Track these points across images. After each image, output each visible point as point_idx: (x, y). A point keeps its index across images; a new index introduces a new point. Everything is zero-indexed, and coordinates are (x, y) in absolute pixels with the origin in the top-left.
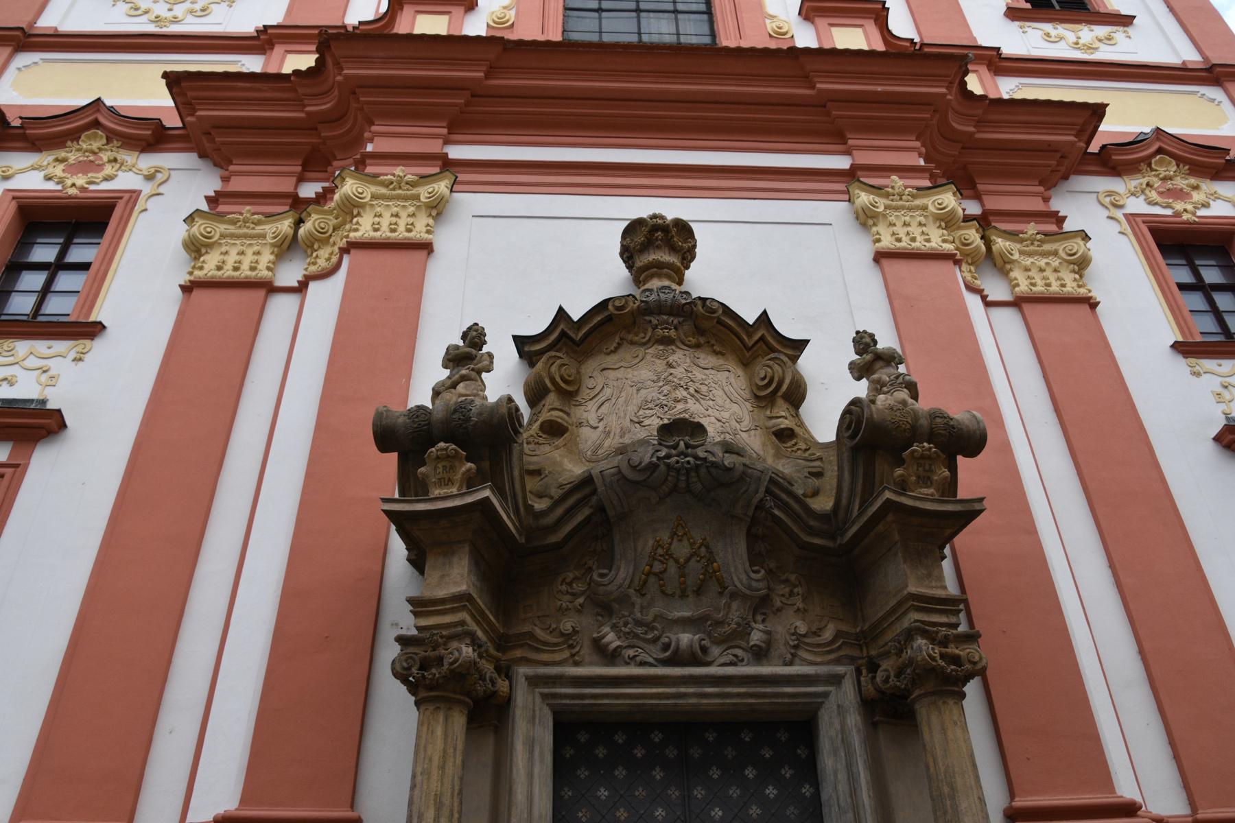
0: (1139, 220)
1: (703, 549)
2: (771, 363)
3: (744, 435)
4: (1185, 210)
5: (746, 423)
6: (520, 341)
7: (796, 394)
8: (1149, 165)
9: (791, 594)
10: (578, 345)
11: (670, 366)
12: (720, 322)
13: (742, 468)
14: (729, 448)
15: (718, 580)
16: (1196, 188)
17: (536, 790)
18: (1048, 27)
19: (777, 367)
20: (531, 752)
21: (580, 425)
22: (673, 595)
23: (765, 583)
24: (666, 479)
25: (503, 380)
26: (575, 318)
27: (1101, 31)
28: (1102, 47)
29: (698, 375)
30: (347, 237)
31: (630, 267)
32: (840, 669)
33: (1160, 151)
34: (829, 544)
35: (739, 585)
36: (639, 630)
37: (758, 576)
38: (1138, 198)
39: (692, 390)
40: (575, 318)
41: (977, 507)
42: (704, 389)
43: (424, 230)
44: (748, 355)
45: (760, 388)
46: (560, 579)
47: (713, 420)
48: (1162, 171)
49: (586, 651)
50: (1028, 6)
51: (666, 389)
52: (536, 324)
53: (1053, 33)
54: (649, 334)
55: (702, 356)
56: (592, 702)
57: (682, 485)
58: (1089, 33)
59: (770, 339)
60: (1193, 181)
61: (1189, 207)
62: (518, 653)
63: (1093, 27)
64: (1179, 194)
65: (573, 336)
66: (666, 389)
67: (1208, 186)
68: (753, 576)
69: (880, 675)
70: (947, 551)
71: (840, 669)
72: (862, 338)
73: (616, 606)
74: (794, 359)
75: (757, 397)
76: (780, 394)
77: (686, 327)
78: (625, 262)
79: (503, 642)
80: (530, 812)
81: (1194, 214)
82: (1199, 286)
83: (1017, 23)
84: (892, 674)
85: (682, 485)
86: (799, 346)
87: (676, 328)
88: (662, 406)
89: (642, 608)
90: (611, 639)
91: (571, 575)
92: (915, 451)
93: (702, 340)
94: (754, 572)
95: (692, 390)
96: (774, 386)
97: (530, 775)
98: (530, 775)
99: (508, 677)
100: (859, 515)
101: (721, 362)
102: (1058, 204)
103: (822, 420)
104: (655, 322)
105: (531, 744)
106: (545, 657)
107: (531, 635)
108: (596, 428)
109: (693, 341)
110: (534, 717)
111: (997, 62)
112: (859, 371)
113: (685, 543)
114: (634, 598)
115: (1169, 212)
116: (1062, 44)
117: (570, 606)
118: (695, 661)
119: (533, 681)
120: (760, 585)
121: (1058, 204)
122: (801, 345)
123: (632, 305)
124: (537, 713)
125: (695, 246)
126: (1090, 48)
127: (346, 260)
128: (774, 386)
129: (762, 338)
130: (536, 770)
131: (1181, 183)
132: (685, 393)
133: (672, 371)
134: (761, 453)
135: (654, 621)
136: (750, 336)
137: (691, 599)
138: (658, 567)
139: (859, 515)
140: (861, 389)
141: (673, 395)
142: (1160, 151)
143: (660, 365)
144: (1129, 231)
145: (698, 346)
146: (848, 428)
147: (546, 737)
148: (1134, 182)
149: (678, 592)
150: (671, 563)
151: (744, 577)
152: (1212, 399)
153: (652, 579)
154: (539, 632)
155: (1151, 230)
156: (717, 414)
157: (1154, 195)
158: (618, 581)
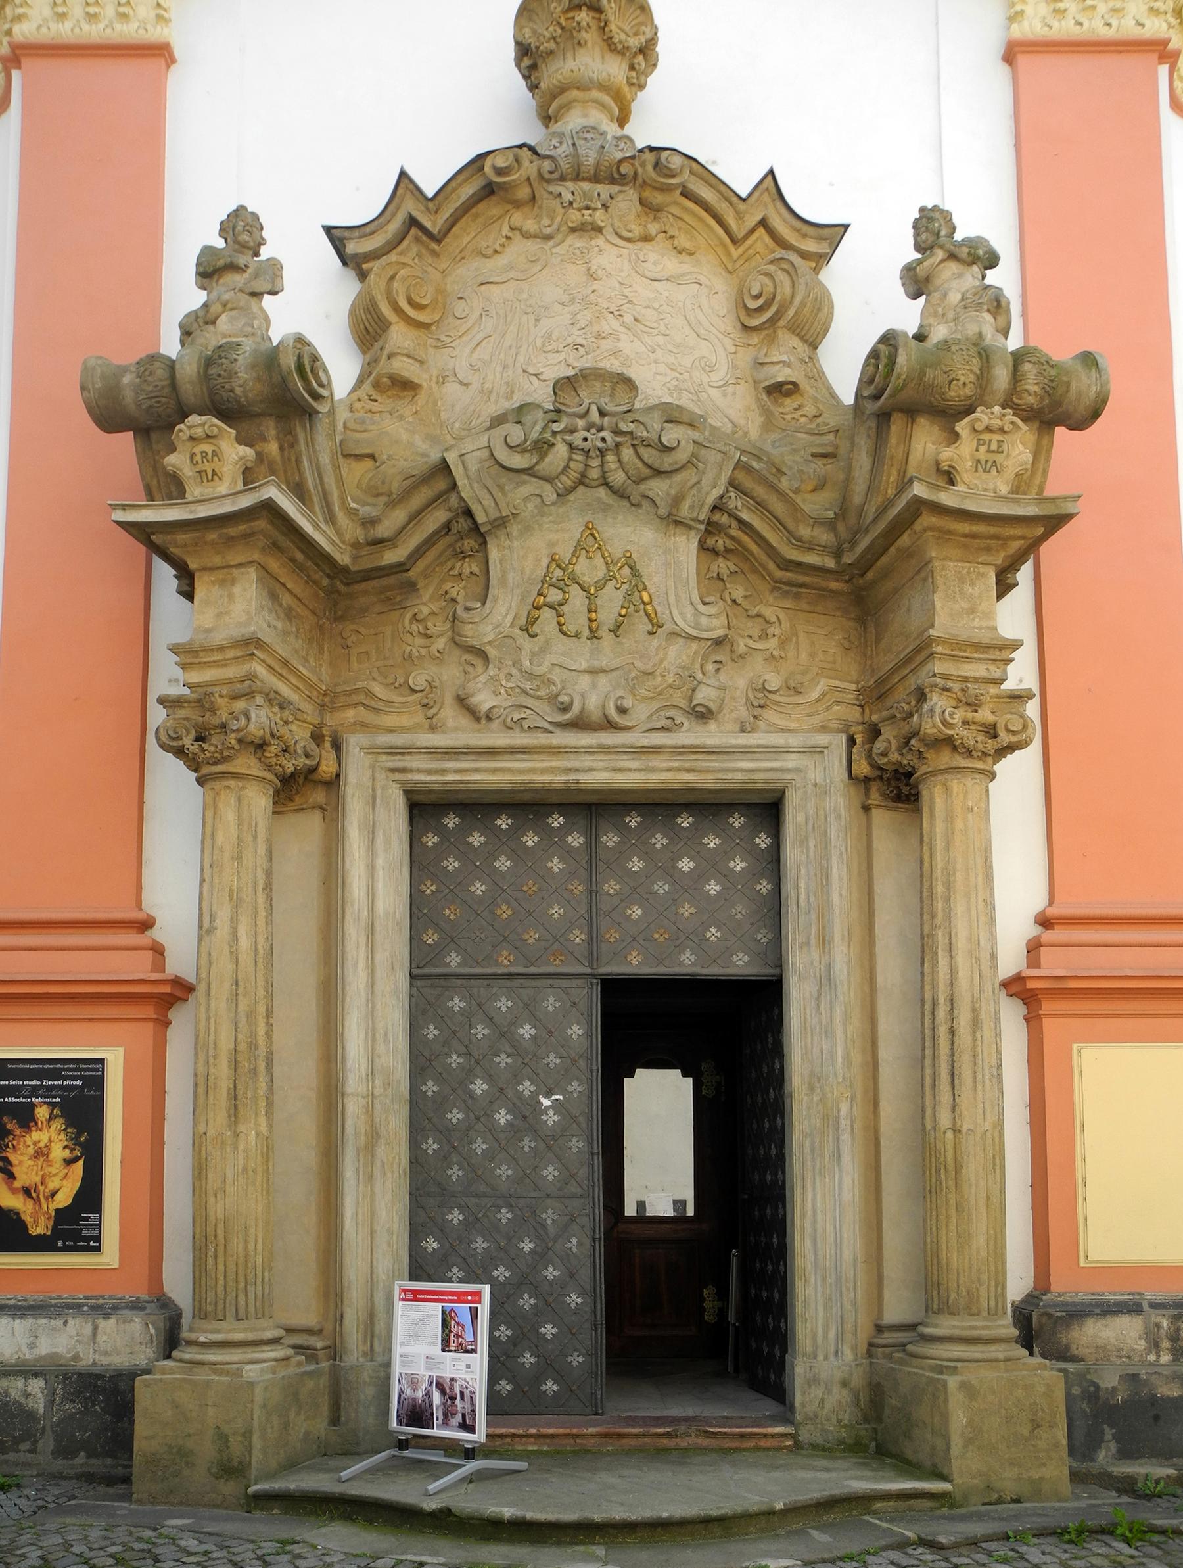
1: (626, 570)
2: (772, 268)
3: (714, 393)
5: (718, 377)
6: (336, 236)
7: (811, 326)
9: (764, 636)
10: (439, 242)
11: (592, 277)
12: (686, 194)
13: (691, 448)
14: (673, 416)
15: (647, 615)
17: (380, 886)
19: (781, 277)
20: (372, 841)
21: (442, 380)
22: (577, 635)
23: (723, 618)
24: (567, 466)
25: (309, 306)
26: (430, 193)
29: (642, 290)
30: (9, 33)
31: (533, 88)
32: (822, 739)
34: (830, 563)
35: (681, 624)
36: (528, 686)
37: (712, 610)
39: (628, 318)
40: (430, 193)
41: (1070, 508)
42: (650, 315)
43: (152, 14)
44: (735, 252)
45: (750, 312)
46: (409, 616)
47: (662, 368)
49: (449, 713)
51: (585, 316)
52: (362, 204)
54: (559, 219)
55: (652, 257)
56: (458, 777)
57: (594, 474)
59: (779, 224)
62: (350, 714)
65: (428, 225)
66: (585, 316)
68: (701, 608)
69: (879, 745)
70: (1025, 574)
71: (822, 739)
72: (931, 219)
73: (492, 652)
74: (822, 259)
75: (745, 328)
76: (782, 323)
77: (623, 205)
78: (524, 77)
79: (328, 701)
80: (372, 909)
84: (894, 744)
85: (594, 474)
86: (835, 233)
87: (605, 207)
88: (577, 347)
89: (533, 654)
90: (484, 700)
91: (425, 610)
92: (978, 420)
93: (653, 228)
94: (704, 604)
95: (628, 318)
96: (774, 309)
97: (371, 868)
98: (371, 868)
99: (337, 746)
100: (876, 520)
101: (686, 267)
103: (842, 367)
104: (567, 196)
105: (371, 832)
106: (390, 720)
107: (369, 693)
108: (466, 385)
109: (637, 230)
110: (374, 798)
112: (916, 282)
113: (599, 561)
114: (520, 641)
117: (423, 651)
118: (610, 725)
119: (374, 751)
120: (715, 622)
122: (835, 233)
123: (529, 167)
124: (379, 792)
125: (652, 41)
127: (16, 75)
128: (774, 309)
129: (763, 223)
130: (380, 862)
132: (615, 324)
133: (596, 285)
134: (742, 422)
135: (550, 671)
136: (739, 216)
137: (607, 639)
138: (554, 596)
139: (876, 520)
140: (907, 316)
141: (596, 328)
143: (574, 274)
145: (646, 238)
146: (871, 381)
147: (394, 821)
149: (586, 633)
150: (575, 590)
151: (689, 612)
153: (547, 613)
154: (378, 689)
156: (671, 359)
158: (497, 617)
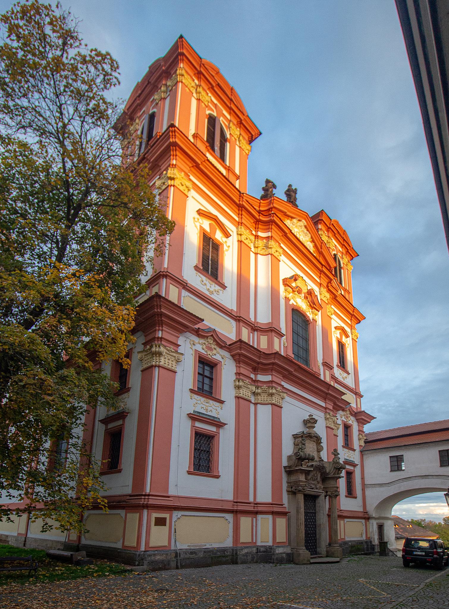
18: (204, 278)
27: (218, 288)
28: (215, 294)
38: (200, 346)
48: (209, 341)
50: (202, 268)
53: (205, 282)
58: (215, 287)
60: (215, 347)
61: (211, 354)
63: (216, 286)
64: (210, 349)
67: (218, 349)
102: (181, 341)
115: (206, 353)
116: (205, 287)
121: (181, 341)
126: (212, 293)
131: (213, 346)
142: (212, 335)
148: (202, 341)
155: (199, 356)
157: (204, 347)
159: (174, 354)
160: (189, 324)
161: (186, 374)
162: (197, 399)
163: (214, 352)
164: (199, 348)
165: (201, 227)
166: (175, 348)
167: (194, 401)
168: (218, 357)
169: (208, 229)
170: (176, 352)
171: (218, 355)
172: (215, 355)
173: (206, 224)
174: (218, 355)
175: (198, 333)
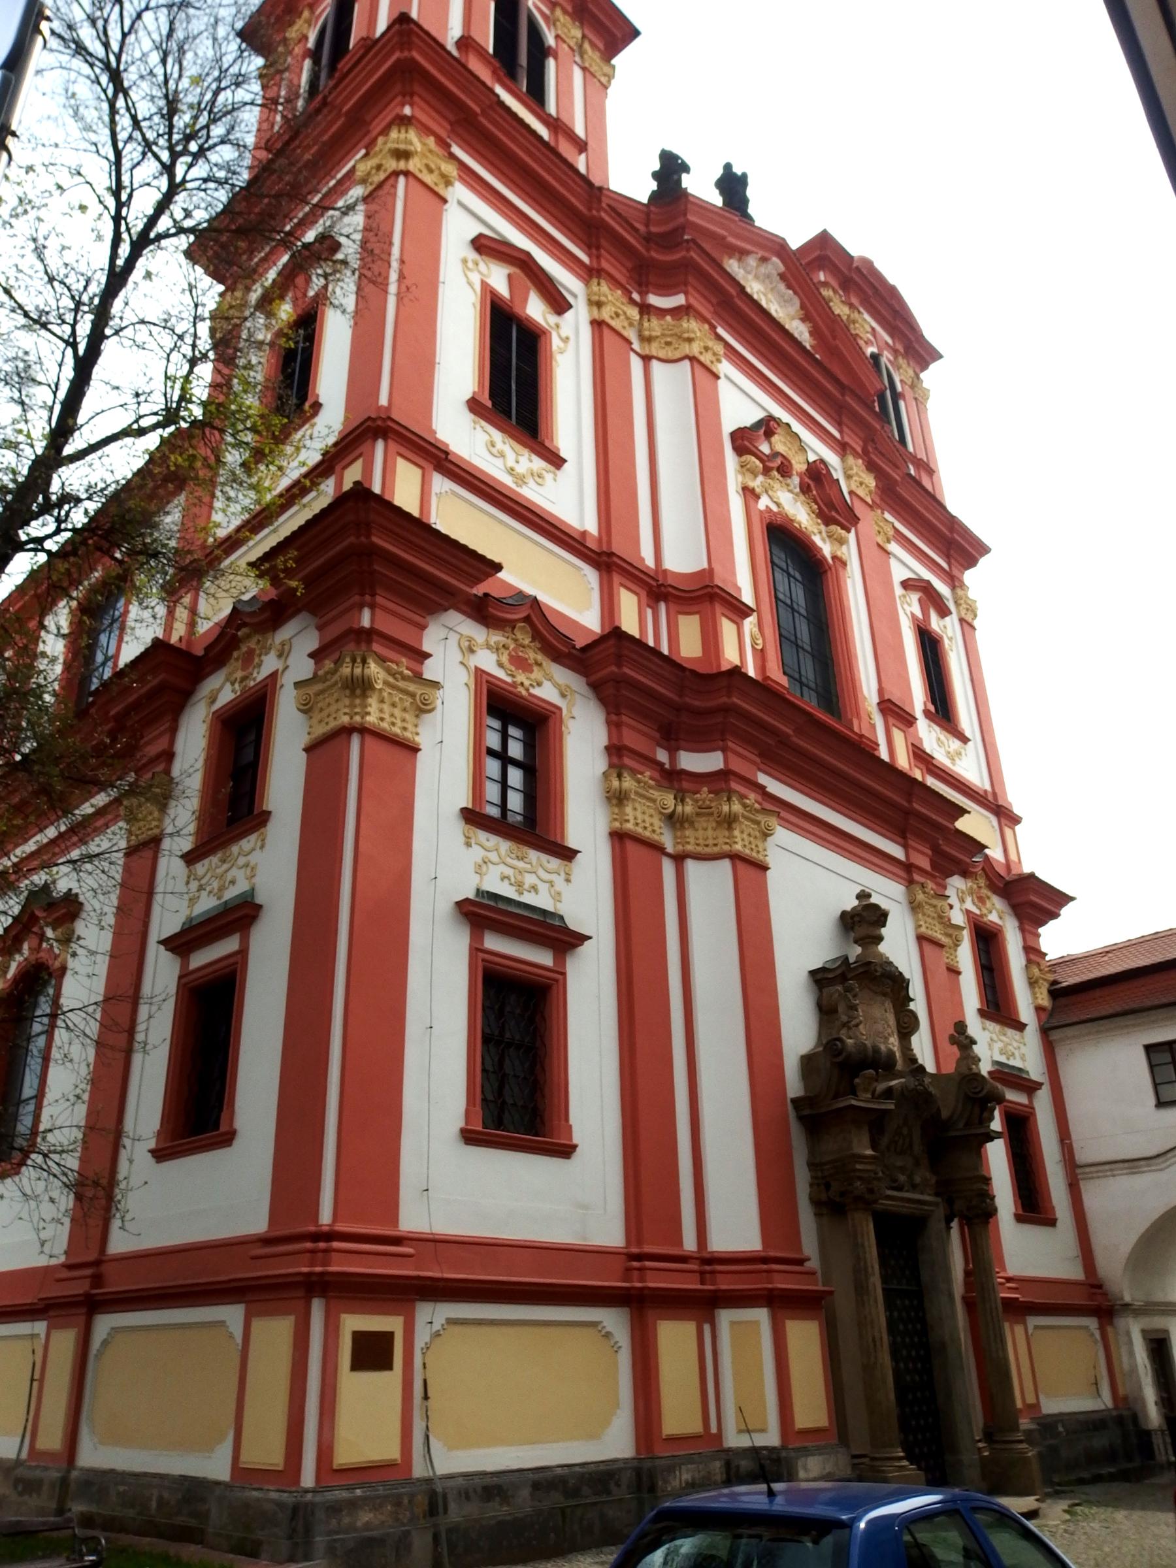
0: (485, 676)
4: (522, 684)
8: (514, 628)
16: (540, 665)
18: (497, 436)
28: (531, 483)
33: (527, 619)
60: (540, 657)
61: (527, 683)
81: (527, 690)
82: (502, 756)
83: (472, 416)
111: (438, 459)
116: (499, 462)
126: (521, 480)
131: (532, 655)
142: (527, 619)
144: (473, 687)
148: (497, 638)
152: (472, 869)
159: (412, 687)
160: (454, 579)
161: (447, 754)
162: (488, 845)
163: (537, 674)
164: (487, 661)
165: (484, 285)
166: (413, 665)
167: (477, 853)
168: (547, 693)
169: (503, 289)
170: (418, 676)
171: (550, 685)
172: (539, 684)
173: (499, 277)
174: (550, 685)
175: (485, 611)
